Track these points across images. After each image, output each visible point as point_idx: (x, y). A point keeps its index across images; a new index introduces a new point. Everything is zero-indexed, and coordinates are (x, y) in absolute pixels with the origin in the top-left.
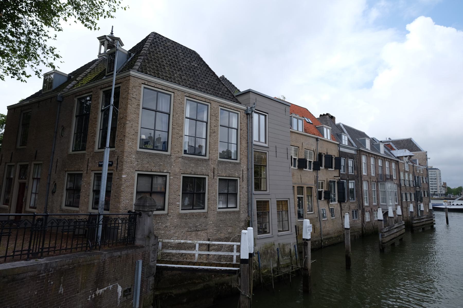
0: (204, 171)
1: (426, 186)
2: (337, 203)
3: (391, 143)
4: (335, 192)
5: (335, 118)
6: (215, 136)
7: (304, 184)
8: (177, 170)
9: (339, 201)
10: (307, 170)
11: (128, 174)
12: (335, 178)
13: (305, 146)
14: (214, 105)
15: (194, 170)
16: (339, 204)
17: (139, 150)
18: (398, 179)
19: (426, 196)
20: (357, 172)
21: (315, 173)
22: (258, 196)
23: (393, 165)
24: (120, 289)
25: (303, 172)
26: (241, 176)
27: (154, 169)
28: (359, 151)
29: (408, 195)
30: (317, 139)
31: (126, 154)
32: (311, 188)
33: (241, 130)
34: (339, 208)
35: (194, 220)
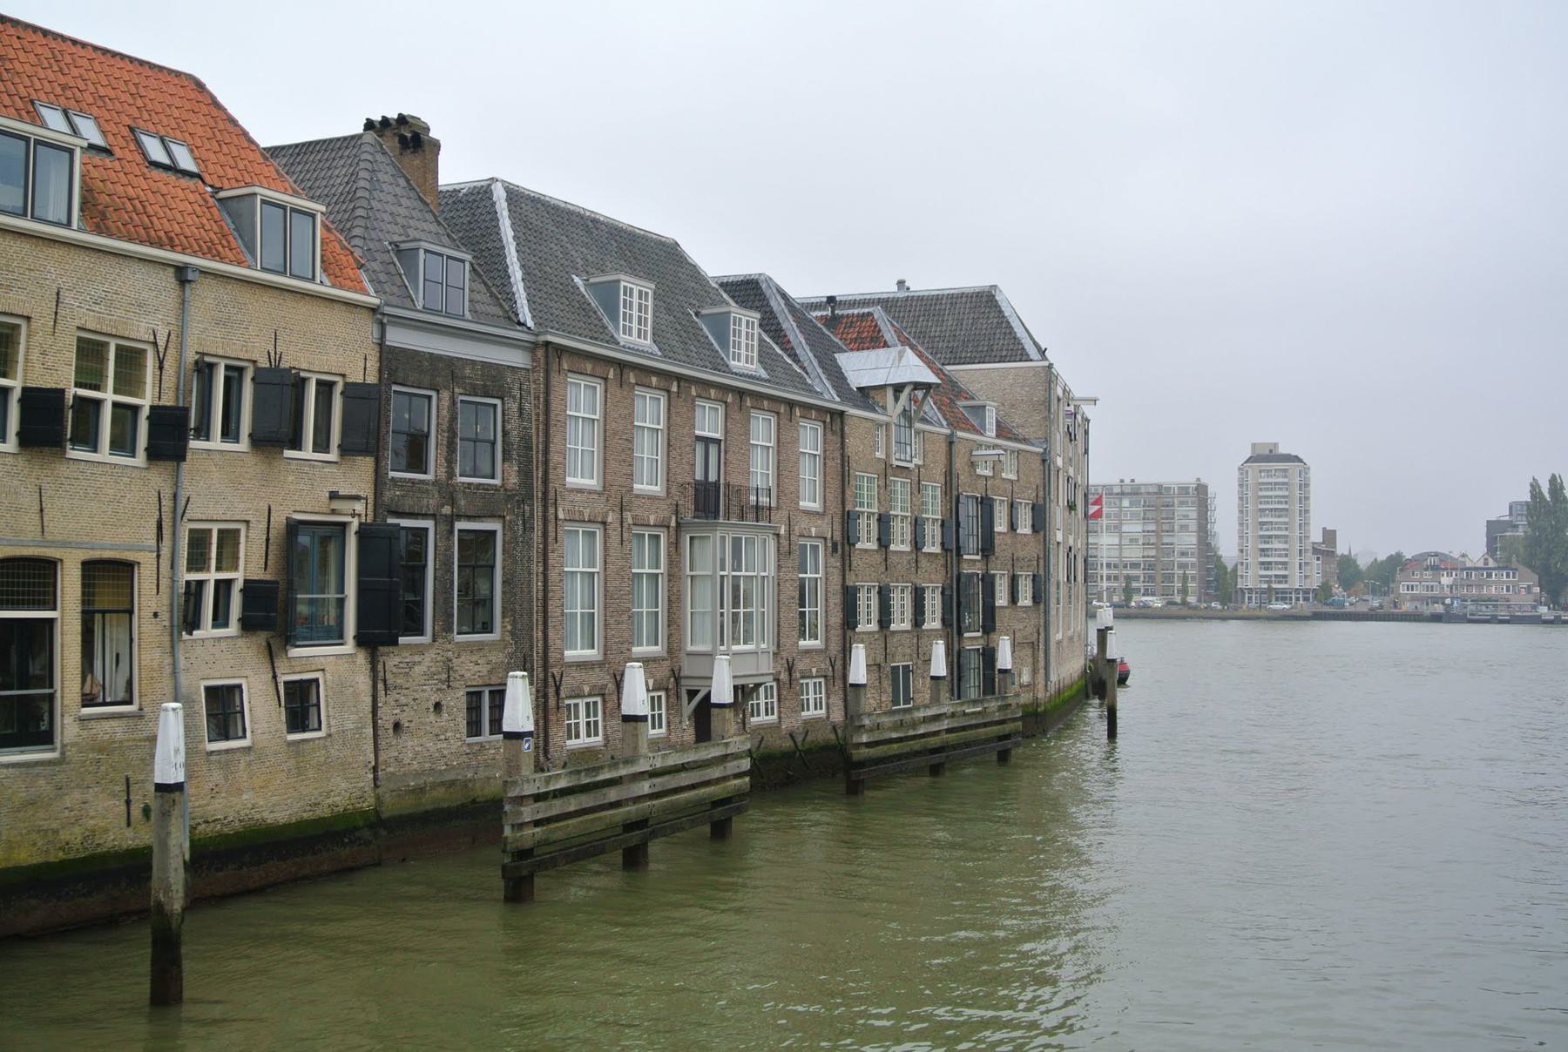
1: (1032, 550)
2: (349, 647)
3: (877, 311)
4: (341, 588)
5: (436, 145)
7: (65, 545)
9: (361, 641)
10: (307, 453)
12: (336, 505)
13: (84, 314)
16: (362, 658)
18: (834, 508)
19: (1025, 600)
20: (526, 473)
21: (159, 479)
23: (810, 438)
25: (63, 469)
28: (540, 353)
29: (901, 604)
30: (182, 274)
34: (363, 681)
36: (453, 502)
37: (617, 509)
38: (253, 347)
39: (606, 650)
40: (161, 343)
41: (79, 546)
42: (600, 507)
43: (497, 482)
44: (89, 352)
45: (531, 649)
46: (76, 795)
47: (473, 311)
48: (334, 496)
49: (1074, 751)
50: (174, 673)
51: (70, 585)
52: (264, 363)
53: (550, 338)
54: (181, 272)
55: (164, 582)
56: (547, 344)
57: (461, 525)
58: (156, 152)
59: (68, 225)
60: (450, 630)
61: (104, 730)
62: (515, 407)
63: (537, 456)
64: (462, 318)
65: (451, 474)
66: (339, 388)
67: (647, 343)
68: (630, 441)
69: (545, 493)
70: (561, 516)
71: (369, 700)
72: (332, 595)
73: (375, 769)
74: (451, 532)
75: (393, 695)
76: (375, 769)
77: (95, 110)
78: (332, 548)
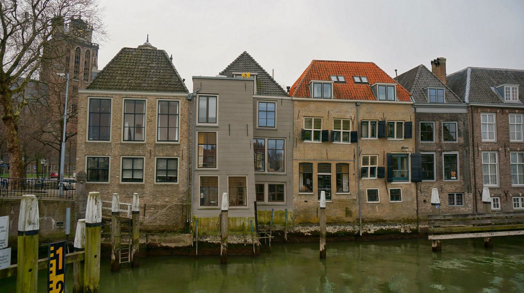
0: (141, 153)
2: (410, 182)
4: (408, 169)
6: (151, 124)
7: (332, 160)
8: (117, 153)
11: (80, 158)
12: (403, 150)
14: (150, 99)
15: (131, 152)
16: (413, 185)
17: (87, 141)
20: (466, 139)
21: (354, 146)
22: (208, 173)
25: (332, 146)
26: (180, 155)
27: (98, 153)
28: (470, 109)
31: (78, 145)
32: (348, 164)
33: (181, 115)
34: (414, 190)
35: (132, 189)
36: (441, 147)
37: (503, 147)
38: (378, 117)
39: (501, 184)
40: (353, 119)
41: (335, 160)
42: (496, 147)
43: (457, 142)
44: (337, 122)
45: (471, 184)
46: (335, 210)
47: (448, 101)
48: (403, 148)
49: (108, 224)
50: (358, 187)
51: (334, 168)
52: (381, 120)
53: (471, 104)
54: (356, 103)
55: (356, 168)
56: (472, 106)
57: (443, 153)
58: (357, 79)
59: (331, 98)
60: (442, 178)
61: (343, 198)
62: (462, 123)
63: (470, 134)
64: (443, 103)
65: (440, 141)
66: (377, 123)
67: (518, 101)
68: (508, 128)
69: (473, 144)
70: (480, 149)
71: (415, 194)
72: (405, 170)
73: (417, 210)
74: (441, 155)
75: (423, 194)
76: (417, 210)
77: (345, 75)
78: (405, 160)
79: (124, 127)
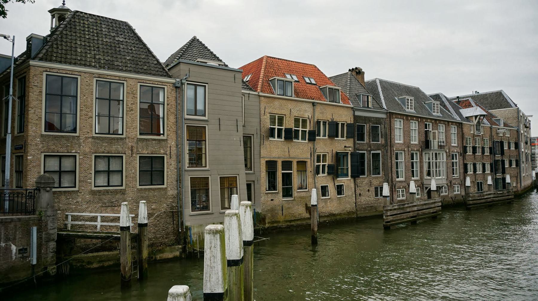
0: (120, 149)
1: (515, 153)
2: (349, 178)
3: (470, 99)
4: (347, 166)
5: (364, 73)
6: (132, 114)
8: (87, 150)
9: (352, 176)
10: (340, 138)
11: (34, 156)
12: (346, 149)
13: (295, 113)
14: (131, 82)
15: (107, 149)
16: (352, 180)
17: (44, 133)
18: (461, 145)
19: (514, 166)
20: (386, 140)
21: (310, 145)
23: (454, 130)
24: (14, 248)
25: (293, 144)
26: (168, 152)
27: (61, 150)
28: (388, 114)
29: (479, 167)
30: (314, 104)
31: (30, 138)
32: (305, 162)
33: (168, 104)
34: (352, 185)
35: (109, 196)
36: (370, 147)
40: (310, 118)
42: (403, 147)
43: (380, 142)
44: (297, 121)
48: (345, 147)
50: (315, 183)
51: (295, 166)
52: (330, 121)
57: (372, 152)
58: (307, 80)
60: (370, 174)
63: (389, 137)
65: (370, 142)
68: (410, 132)
72: (345, 167)
75: (359, 188)
78: (345, 158)
79: (123, 117)
